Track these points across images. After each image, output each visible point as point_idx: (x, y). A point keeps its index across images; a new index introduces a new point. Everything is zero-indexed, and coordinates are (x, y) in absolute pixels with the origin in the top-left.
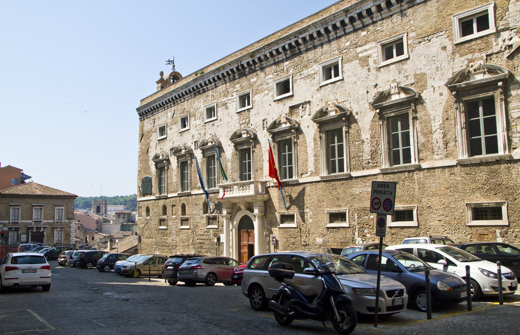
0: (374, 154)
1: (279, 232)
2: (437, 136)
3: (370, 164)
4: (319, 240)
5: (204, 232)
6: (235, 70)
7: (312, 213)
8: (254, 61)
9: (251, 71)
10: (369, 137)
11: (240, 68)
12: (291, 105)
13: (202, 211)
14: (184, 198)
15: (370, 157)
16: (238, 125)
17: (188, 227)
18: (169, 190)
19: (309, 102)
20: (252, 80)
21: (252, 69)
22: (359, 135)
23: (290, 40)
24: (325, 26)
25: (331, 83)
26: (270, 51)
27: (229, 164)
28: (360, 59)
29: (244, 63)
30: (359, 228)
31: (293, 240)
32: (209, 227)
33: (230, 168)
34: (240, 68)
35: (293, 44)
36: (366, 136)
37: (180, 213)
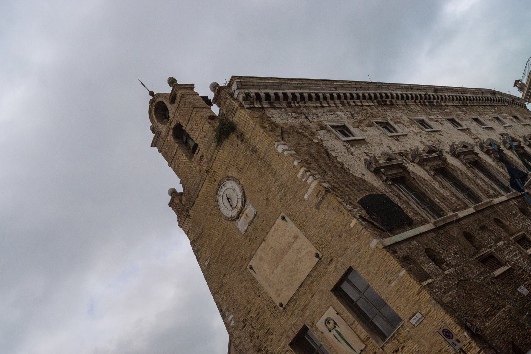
20: (446, 110)
37: (504, 234)
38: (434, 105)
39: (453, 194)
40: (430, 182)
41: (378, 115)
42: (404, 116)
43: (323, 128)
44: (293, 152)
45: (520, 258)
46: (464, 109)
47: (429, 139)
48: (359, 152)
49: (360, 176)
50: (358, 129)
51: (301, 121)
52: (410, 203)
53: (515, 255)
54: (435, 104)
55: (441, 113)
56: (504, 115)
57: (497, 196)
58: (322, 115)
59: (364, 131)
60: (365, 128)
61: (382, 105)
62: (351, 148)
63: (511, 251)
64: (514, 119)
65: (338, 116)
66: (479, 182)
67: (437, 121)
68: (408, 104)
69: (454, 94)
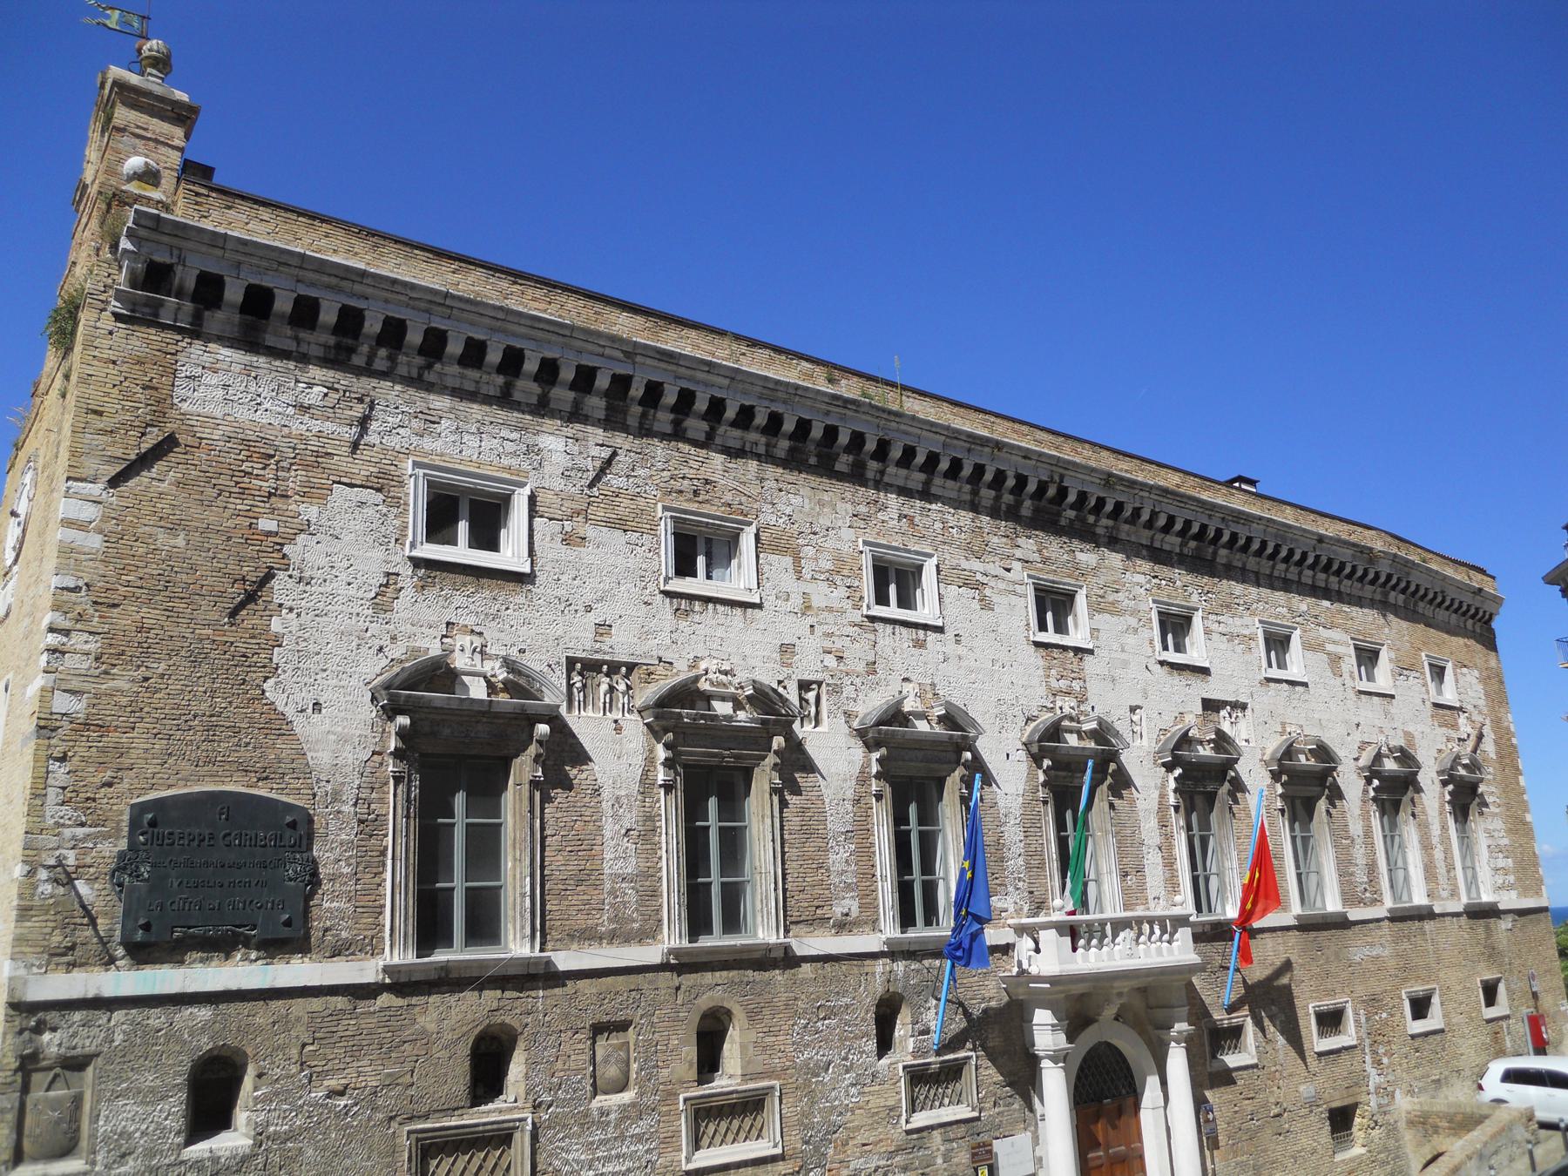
2: (1438, 854)
8: (1101, 502)
12: (1206, 696)
16: (1042, 691)
18: (554, 923)
19: (1244, 707)
20: (1081, 556)
21: (1083, 520)
32: (921, 1119)
33: (1019, 848)
39: (648, 875)
41: (728, 497)
43: (383, 483)
44: (95, 542)
47: (838, 645)
49: (290, 712)
51: (316, 425)
54: (1063, 522)
59: (567, 540)
60: (589, 531)
62: (408, 594)
63: (622, 1138)
64: (1350, 661)
66: (839, 856)
67: (978, 586)
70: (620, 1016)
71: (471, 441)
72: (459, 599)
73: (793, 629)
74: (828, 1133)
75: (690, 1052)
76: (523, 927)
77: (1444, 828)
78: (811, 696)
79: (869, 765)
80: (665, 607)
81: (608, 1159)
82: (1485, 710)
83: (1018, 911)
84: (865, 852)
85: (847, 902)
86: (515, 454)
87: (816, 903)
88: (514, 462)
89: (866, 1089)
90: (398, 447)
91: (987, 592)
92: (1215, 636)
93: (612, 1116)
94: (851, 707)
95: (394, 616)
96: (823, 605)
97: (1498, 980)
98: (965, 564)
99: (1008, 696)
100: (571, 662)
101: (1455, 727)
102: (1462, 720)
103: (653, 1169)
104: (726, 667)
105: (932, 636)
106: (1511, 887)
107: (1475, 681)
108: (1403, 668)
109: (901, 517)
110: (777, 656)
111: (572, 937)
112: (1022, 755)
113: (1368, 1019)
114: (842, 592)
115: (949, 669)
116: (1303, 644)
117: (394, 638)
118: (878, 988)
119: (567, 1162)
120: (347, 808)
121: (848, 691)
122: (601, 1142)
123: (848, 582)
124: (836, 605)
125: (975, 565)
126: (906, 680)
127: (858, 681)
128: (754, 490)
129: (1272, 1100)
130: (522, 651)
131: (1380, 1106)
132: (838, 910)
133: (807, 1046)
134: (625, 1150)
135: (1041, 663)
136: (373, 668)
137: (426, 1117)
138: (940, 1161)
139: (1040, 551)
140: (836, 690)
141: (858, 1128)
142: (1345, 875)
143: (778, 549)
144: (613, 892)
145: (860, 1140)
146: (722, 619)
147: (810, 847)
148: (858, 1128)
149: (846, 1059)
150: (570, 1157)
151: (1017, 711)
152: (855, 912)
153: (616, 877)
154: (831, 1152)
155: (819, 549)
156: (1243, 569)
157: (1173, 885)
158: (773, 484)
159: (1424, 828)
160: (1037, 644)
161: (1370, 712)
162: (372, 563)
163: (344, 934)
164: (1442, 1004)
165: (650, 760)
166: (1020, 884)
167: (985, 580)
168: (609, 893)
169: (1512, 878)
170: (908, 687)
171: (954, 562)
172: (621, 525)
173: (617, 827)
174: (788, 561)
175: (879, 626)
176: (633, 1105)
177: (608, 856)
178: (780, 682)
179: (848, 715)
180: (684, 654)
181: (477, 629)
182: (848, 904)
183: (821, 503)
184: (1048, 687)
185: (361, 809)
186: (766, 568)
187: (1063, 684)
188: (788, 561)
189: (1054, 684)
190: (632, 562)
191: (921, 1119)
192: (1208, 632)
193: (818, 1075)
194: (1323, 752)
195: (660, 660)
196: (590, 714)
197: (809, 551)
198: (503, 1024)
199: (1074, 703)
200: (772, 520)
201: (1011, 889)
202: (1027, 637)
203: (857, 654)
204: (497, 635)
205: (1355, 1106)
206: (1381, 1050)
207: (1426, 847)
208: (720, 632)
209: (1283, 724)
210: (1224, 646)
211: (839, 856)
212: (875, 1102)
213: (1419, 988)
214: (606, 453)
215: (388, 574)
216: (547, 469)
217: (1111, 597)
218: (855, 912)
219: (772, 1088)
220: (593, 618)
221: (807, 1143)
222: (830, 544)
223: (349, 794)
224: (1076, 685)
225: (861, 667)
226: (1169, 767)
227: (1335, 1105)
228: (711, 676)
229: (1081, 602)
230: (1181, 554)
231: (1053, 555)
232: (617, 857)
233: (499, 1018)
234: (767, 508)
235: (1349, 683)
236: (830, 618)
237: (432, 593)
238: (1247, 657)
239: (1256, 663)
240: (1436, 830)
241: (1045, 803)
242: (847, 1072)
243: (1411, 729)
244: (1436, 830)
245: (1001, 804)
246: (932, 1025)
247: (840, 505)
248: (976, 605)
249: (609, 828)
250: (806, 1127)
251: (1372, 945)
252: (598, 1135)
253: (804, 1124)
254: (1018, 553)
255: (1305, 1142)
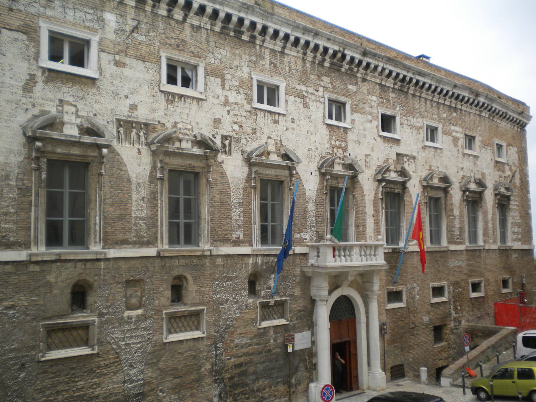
0: (461, 230)
1: (387, 315)
2: (490, 225)
3: (459, 240)
4: (426, 319)
5: (252, 339)
6: (331, 52)
7: (418, 288)
8: (360, 62)
9: (349, 72)
10: (458, 214)
11: (339, 55)
12: (398, 152)
13: (246, 293)
14: (182, 262)
15: (458, 234)
16: (328, 146)
17: (197, 334)
19: (414, 158)
20: (350, 87)
21: (351, 69)
22: (452, 211)
23: (408, 72)
24: (437, 85)
25: (434, 147)
26: (385, 66)
27: (311, 207)
28: (453, 137)
29: (349, 53)
30: (454, 302)
31: (401, 324)
32: (265, 324)
33: (313, 213)
34: (339, 55)
35: (408, 79)
36: (456, 212)
38: (339, 71)
40: (133, 186)
41: (192, 49)
42: (246, 70)
45: (140, 342)
46: (392, 95)
47: (240, 120)
48: (50, 95)
50: (111, 57)
52: (33, 208)
53: (138, 336)
54: (343, 70)
55: (334, 87)
56: (453, 128)
57: (237, 243)
58: (63, 7)
59: (117, 64)
60: (127, 61)
61: (228, 35)
63: (137, 329)
65: (101, 20)
66: (236, 213)
67: (304, 97)
68: (286, 51)
69: (396, 70)
70: (138, 277)
71: (70, 13)
72: (65, 89)
73: (220, 112)
74: (226, 328)
75: (168, 293)
76: (95, 238)
77: (494, 214)
78: (227, 142)
79: (251, 175)
80: (162, 99)
81: (131, 337)
82: (517, 165)
83: (311, 240)
84: (247, 212)
85: (238, 233)
86: (91, 21)
87: (225, 233)
88: (90, 24)
89: (243, 311)
90: (33, 12)
91: (307, 100)
92: (405, 126)
93: (133, 320)
94: (245, 148)
95: (34, 95)
96: (234, 102)
97: (509, 278)
98: (298, 87)
99: (313, 148)
100: (118, 120)
101: (503, 171)
102: (507, 168)
103: (151, 342)
104: (189, 127)
105: (281, 118)
106: (519, 240)
107: (515, 152)
108: (486, 144)
109: (271, 63)
110: (212, 124)
111: (117, 243)
112: (317, 173)
113: (453, 291)
114: (242, 96)
115: (288, 134)
116: (442, 131)
117: (34, 106)
118: (250, 269)
119: (113, 338)
120: (13, 183)
121: (243, 141)
122: (128, 330)
123: (245, 92)
124: (239, 102)
125: (303, 88)
126: (269, 138)
127: (248, 137)
128: (204, 46)
129: (411, 322)
130: (95, 115)
131: (455, 326)
132: (234, 236)
133: (218, 292)
134: (138, 334)
135: (328, 133)
136: (22, 118)
137: (50, 319)
138: (272, 341)
139: (332, 83)
140: (238, 140)
141: (238, 327)
142: (450, 231)
143: (216, 75)
144: (136, 225)
145: (239, 331)
146: (187, 105)
147: (223, 209)
148: (238, 327)
149: (235, 298)
150: (114, 336)
151: (317, 154)
152: (242, 237)
153: (136, 218)
154: (226, 336)
155: (233, 76)
156: (420, 97)
157: (377, 231)
158: (213, 44)
159: (485, 214)
160: (328, 125)
161: (468, 164)
162: (22, 69)
163: (11, 239)
164: (485, 286)
165: (154, 167)
166: (313, 229)
167: (306, 94)
168: (134, 225)
169: (520, 236)
170: (269, 140)
171: (293, 86)
172: (142, 58)
173: (138, 196)
174: (219, 80)
175: (258, 112)
176: (142, 315)
177: (133, 209)
178: (213, 135)
179: (243, 152)
180: (170, 120)
181: (73, 103)
182: (239, 234)
183: (234, 54)
184: (331, 144)
185: (20, 184)
186: (209, 83)
187: (338, 143)
188: (219, 80)
189: (333, 143)
190: (148, 77)
191: (265, 324)
192: (402, 124)
193: (222, 305)
194: (445, 179)
195: (159, 122)
196: (127, 145)
197: (228, 77)
198: (85, 280)
199: (341, 152)
200: (212, 60)
201: (309, 230)
202: (323, 122)
203: (248, 125)
204: (83, 107)
205: (445, 325)
206: (458, 304)
207: (486, 222)
208: (186, 111)
209: (430, 166)
210: (408, 130)
211: (236, 213)
212: (246, 316)
213: (476, 280)
214: (135, 23)
215: (30, 75)
216: (107, 29)
217: (361, 106)
218: (242, 237)
219: (203, 310)
220: (128, 102)
221: (217, 332)
222: (238, 74)
223: (13, 176)
224: (343, 144)
225: (249, 131)
226: (380, 181)
227: (436, 325)
228: (182, 131)
229: (348, 107)
230: (393, 88)
231: (337, 85)
232: (138, 208)
233: (83, 277)
234: (210, 55)
235: (461, 150)
236: (236, 108)
237: (51, 85)
238: (419, 136)
239: (421, 138)
240: (490, 215)
241: (326, 194)
242: (235, 304)
243: (484, 171)
244: (490, 215)
245: (307, 194)
246: (272, 286)
247: (243, 56)
248: (301, 106)
249: (134, 196)
250: (217, 326)
251: (458, 261)
252: (127, 327)
253: (216, 324)
254: (322, 83)
255: (423, 338)
